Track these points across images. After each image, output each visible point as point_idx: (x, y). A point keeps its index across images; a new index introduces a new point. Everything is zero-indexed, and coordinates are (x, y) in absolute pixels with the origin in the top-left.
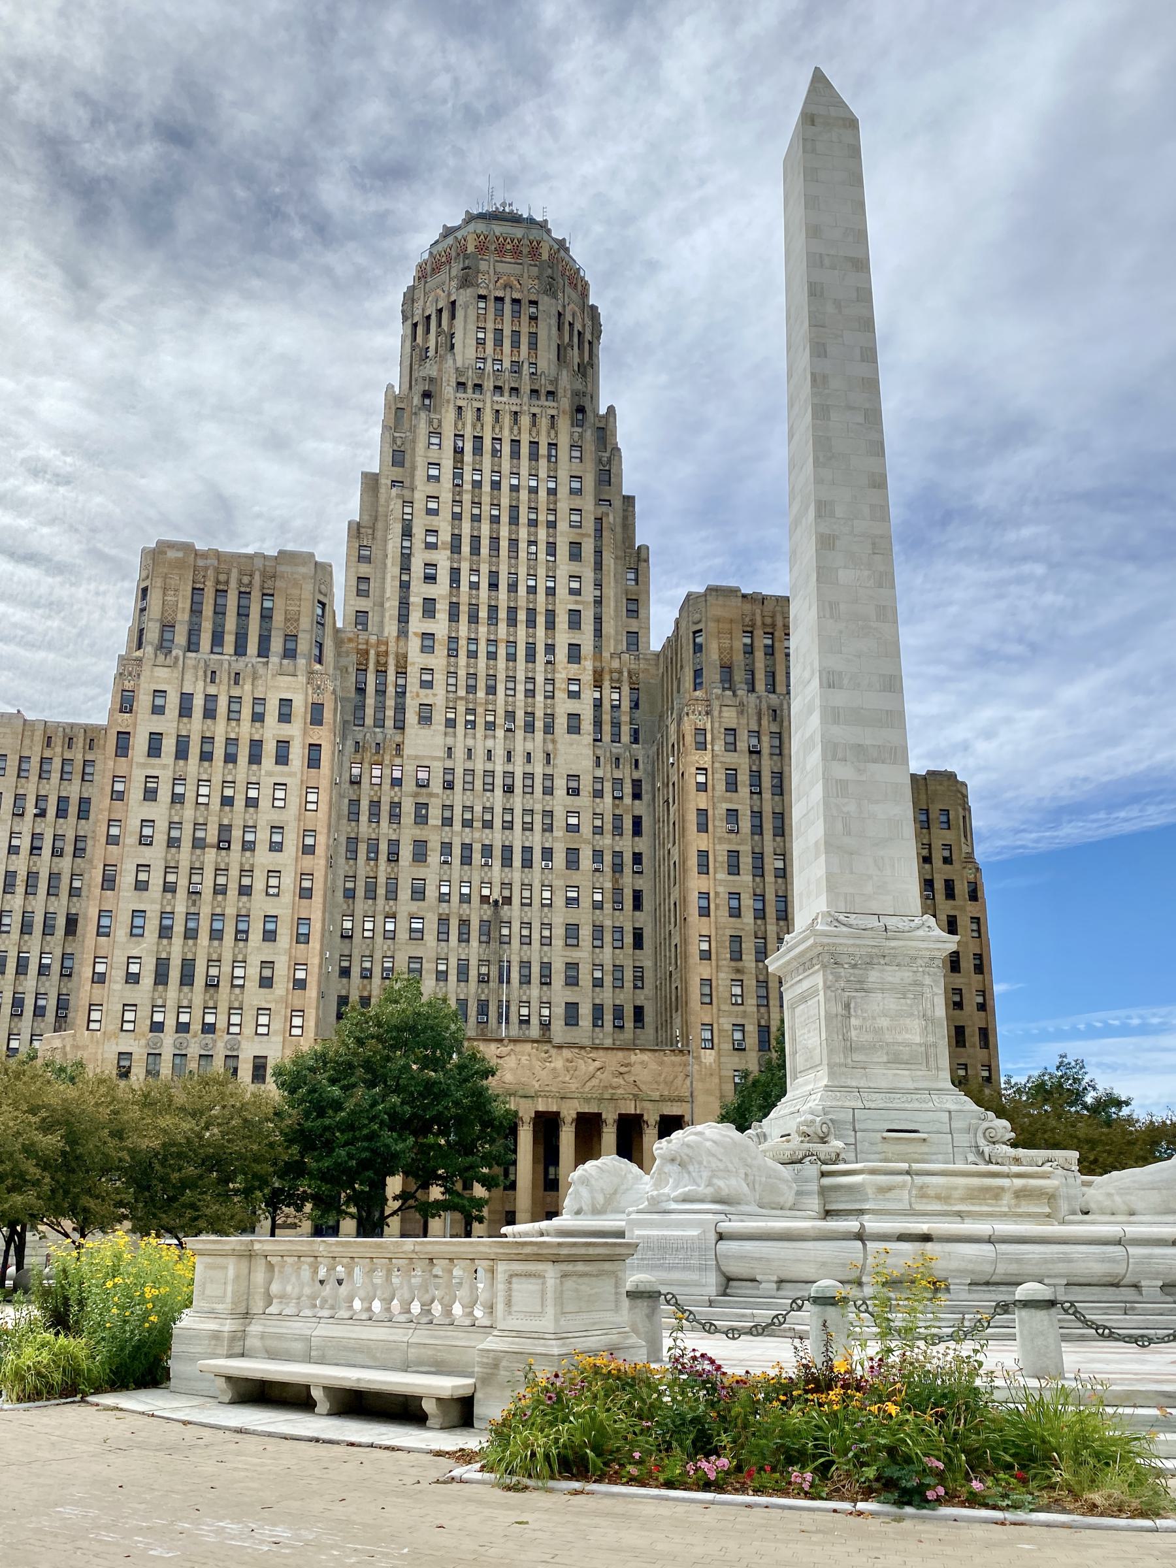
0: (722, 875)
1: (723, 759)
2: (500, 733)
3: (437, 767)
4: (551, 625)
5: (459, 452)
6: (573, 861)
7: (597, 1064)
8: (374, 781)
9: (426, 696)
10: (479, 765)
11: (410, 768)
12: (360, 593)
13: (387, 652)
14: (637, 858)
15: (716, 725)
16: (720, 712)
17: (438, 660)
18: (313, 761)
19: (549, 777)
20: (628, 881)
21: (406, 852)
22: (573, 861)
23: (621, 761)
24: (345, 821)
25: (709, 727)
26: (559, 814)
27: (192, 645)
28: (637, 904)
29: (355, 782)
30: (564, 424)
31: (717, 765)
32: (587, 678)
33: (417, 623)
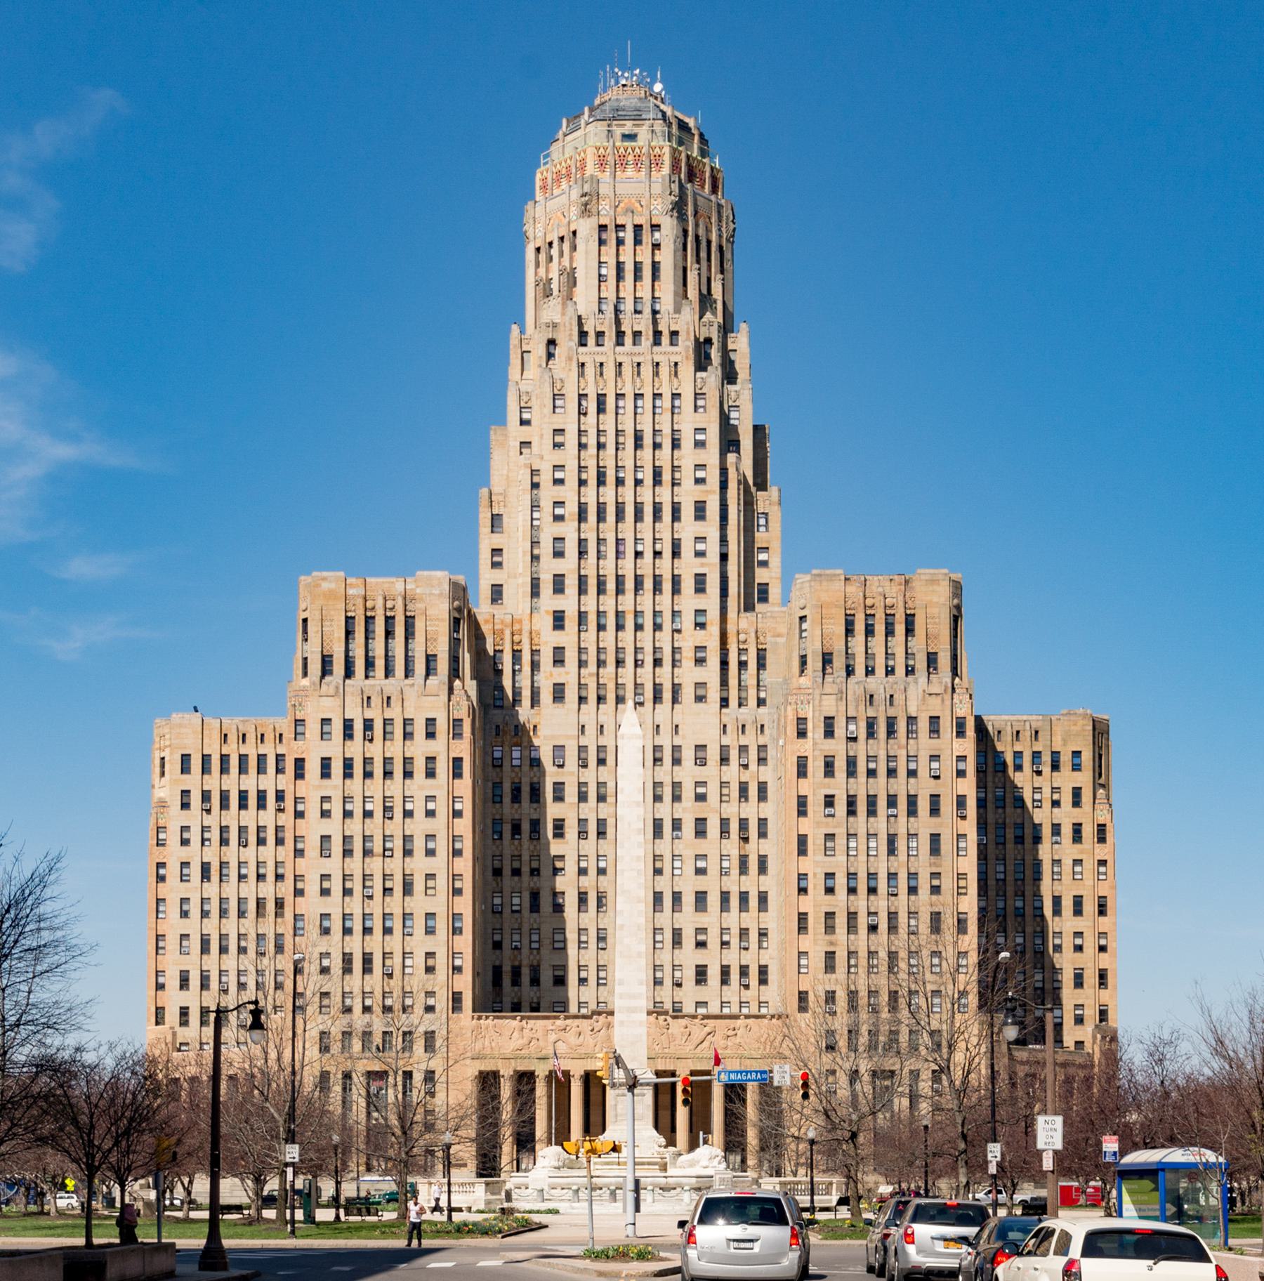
0: (820, 857)
1: (823, 747)
7: (707, 1029)
8: (515, 762)
13: (521, 630)
14: (762, 823)
15: (817, 714)
16: (821, 701)
17: (567, 638)
19: (676, 749)
20: (752, 849)
23: (747, 727)
24: (490, 804)
25: (810, 716)
27: (349, 673)
28: (763, 869)
29: (497, 765)
30: (687, 368)
31: (817, 753)
33: (549, 601)
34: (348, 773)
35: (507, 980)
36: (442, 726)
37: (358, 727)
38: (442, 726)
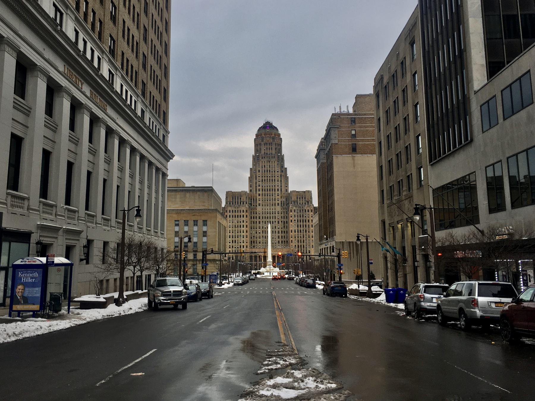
2: (269, 206)
3: (261, 211)
4: (275, 191)
5: (262, 167)
6: (278, 222)
9: (259, 202)
10: (266, 211)
11: (258, 212)
12: (251, 187)
14: (287, 222)
17: (261, 197)
18: (247, 217)
19: (275, 212)
21: (258, 223)
22: (278, 222)
26: (277, 216)
32: (280, 198)
33: (258, 192)
34: (233, 217)
35: (253, 243)
36: (245, 211)
37: (234, 211)
38: (245, 211)
